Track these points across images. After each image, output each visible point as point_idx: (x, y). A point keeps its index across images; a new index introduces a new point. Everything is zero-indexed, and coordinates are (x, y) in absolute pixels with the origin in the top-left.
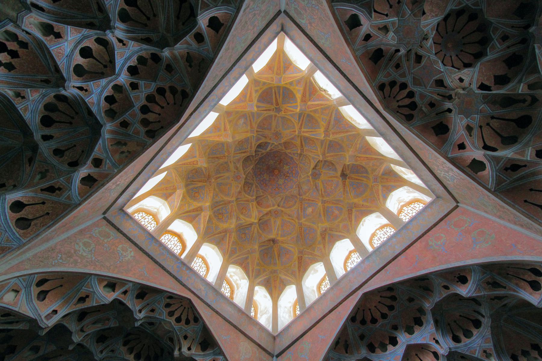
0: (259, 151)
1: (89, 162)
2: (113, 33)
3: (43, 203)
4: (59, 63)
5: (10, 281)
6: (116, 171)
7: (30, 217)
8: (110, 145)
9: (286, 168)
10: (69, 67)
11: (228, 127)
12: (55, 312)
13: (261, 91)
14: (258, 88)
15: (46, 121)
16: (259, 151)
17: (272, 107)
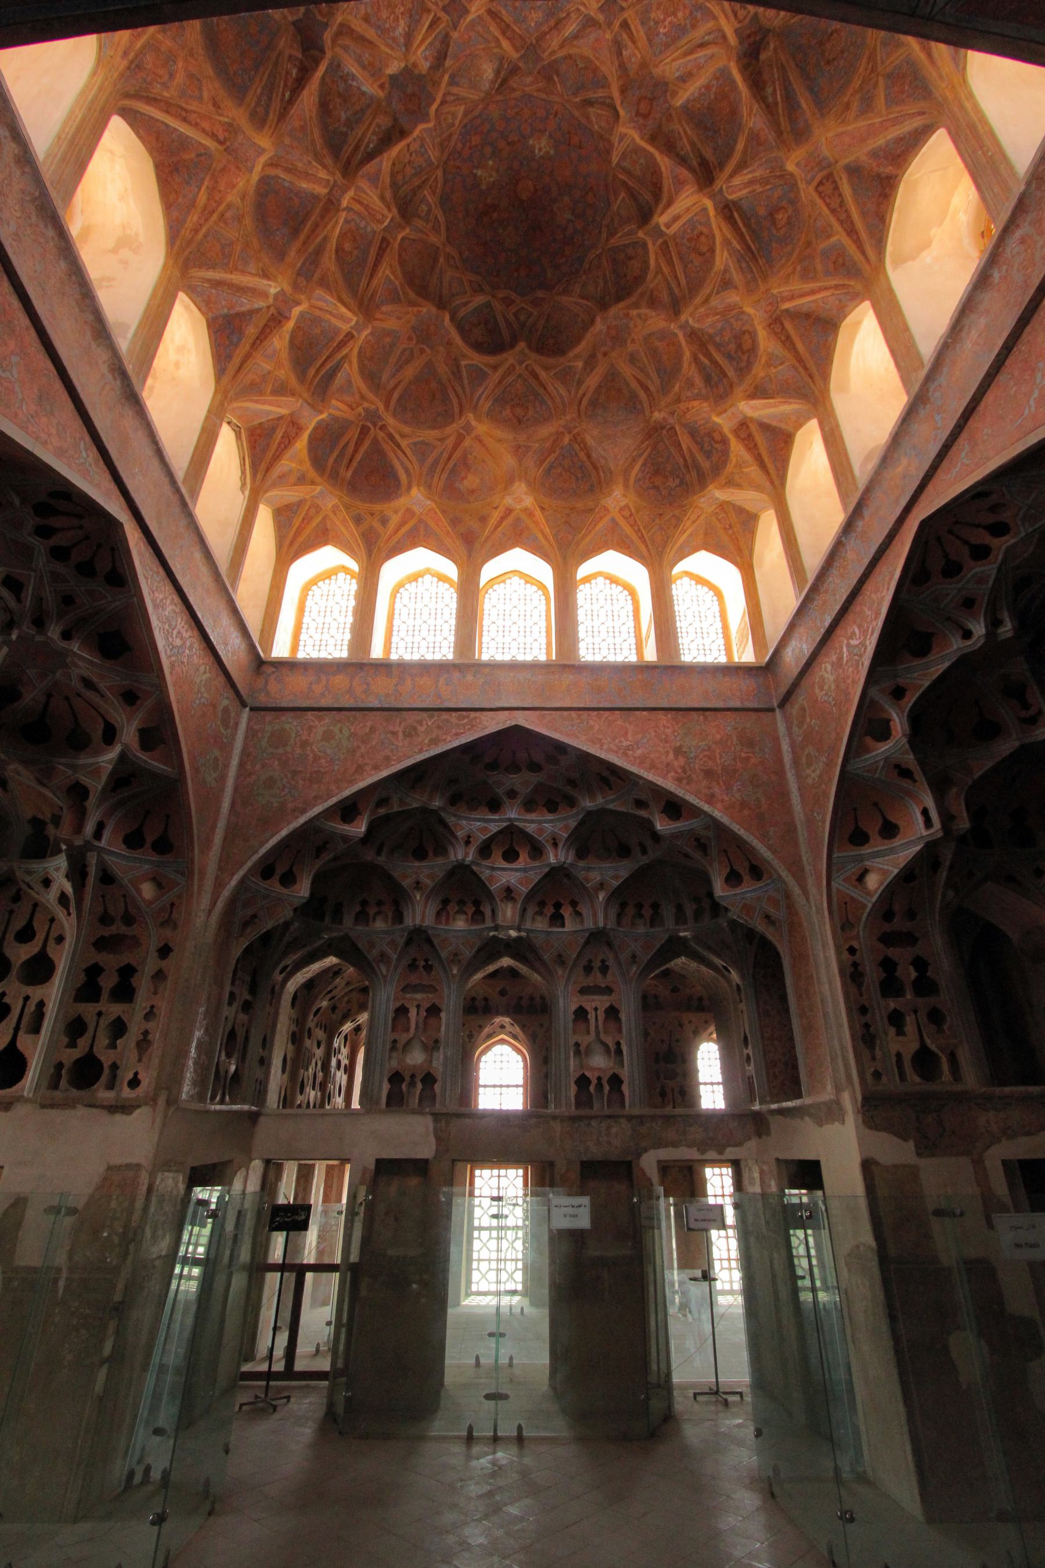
0: (509, 324)
1: (643, 813)
2: (463, 860)
3: (725, 851)
4: (537, 880)
5: (834, 890)
6: (641, 782)
7: (747, 864)
8: (610, 792)
9: (487, 174)
10: (535, 868)
11: (496, 515)
12: (925, 812)
13: (377, 507)
14: (376, 524)
15: (624, 851)
16: (509, 324)
17: (381, 435)
